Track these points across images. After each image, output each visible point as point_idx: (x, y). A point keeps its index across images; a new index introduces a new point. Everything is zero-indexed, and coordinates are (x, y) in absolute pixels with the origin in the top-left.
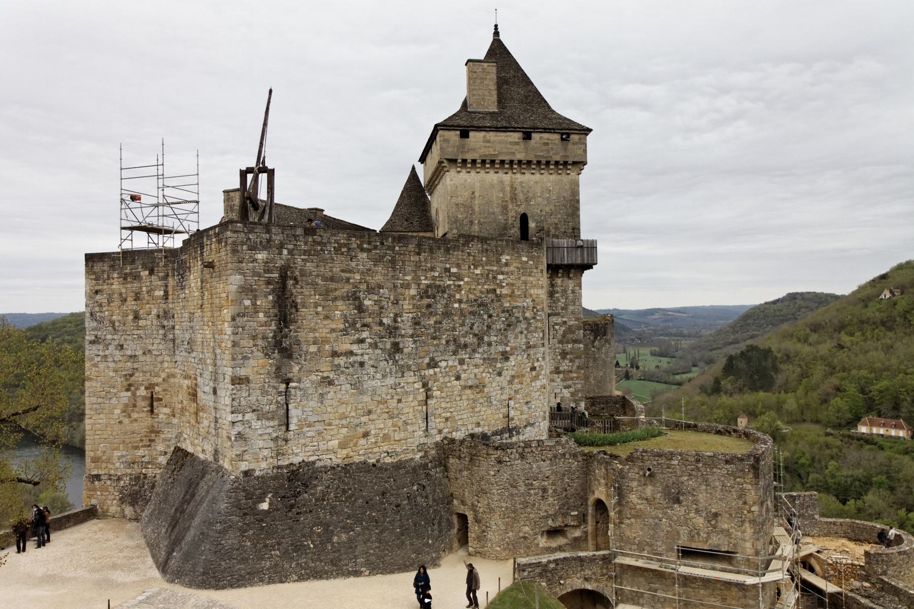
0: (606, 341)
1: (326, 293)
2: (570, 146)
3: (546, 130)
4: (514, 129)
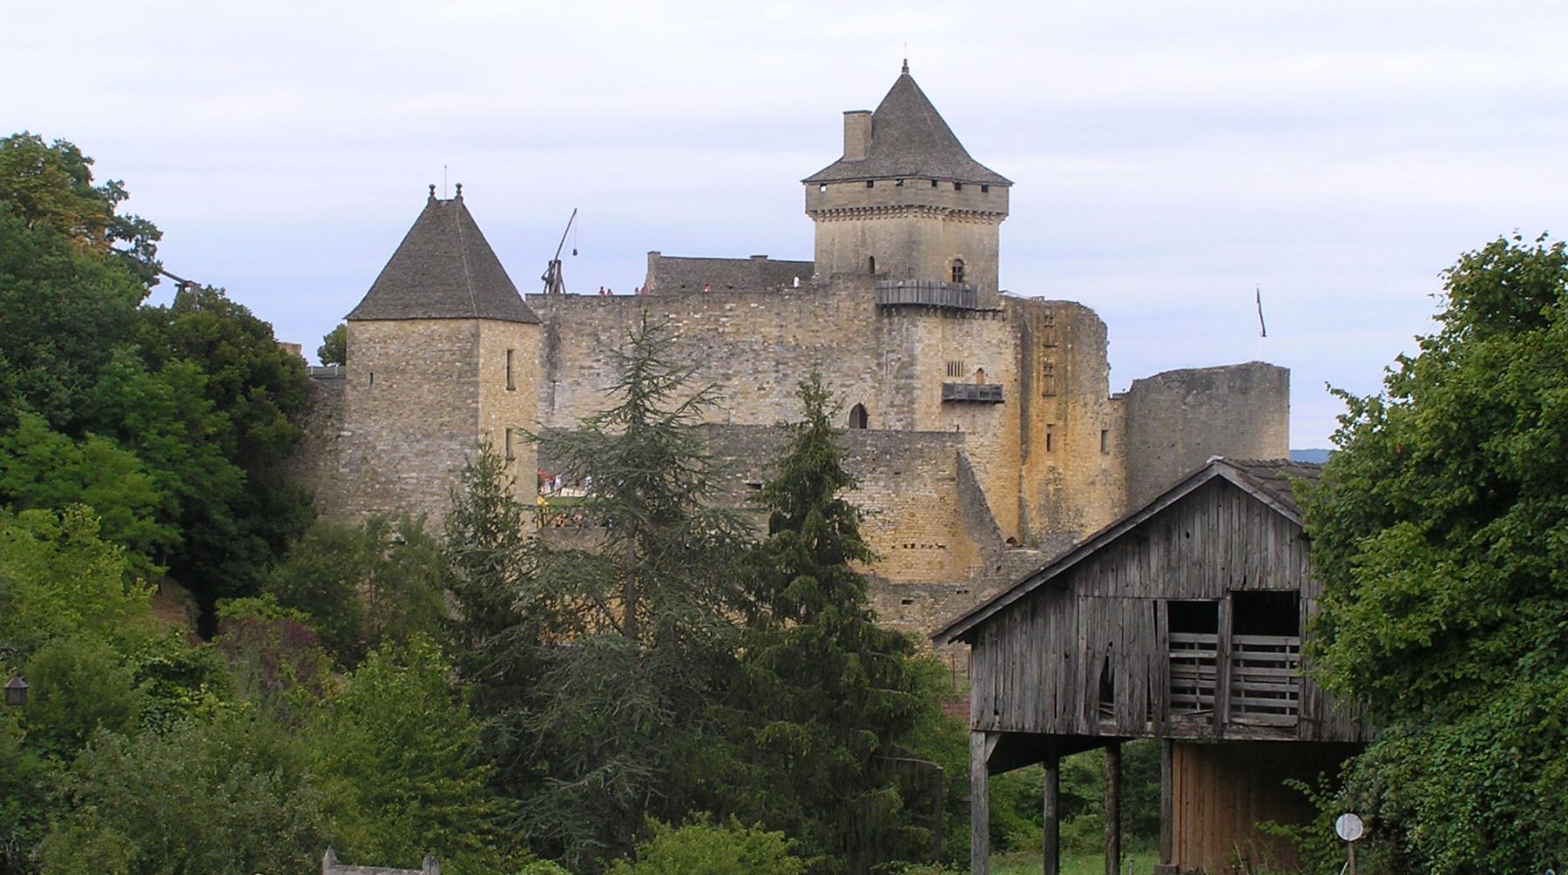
0: (1210, 397)
1: (577, 332)
2: (903, 189)
3: (883, 178)
4: (858, 180)
